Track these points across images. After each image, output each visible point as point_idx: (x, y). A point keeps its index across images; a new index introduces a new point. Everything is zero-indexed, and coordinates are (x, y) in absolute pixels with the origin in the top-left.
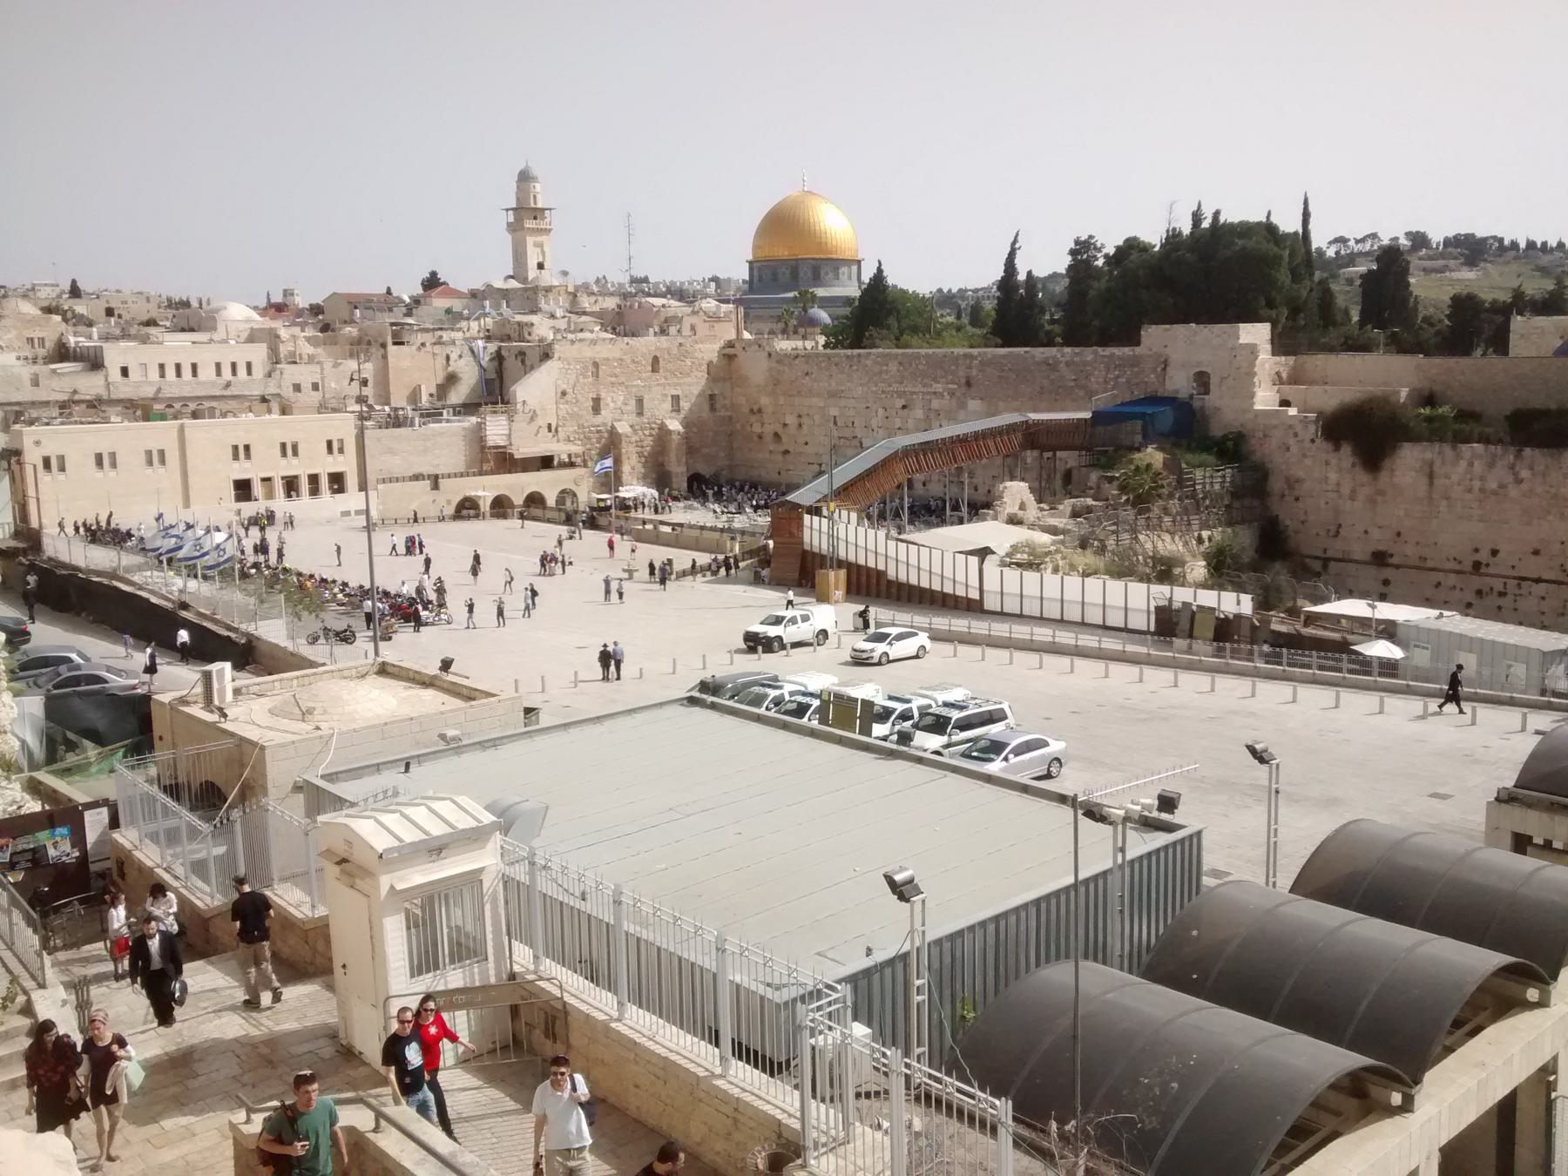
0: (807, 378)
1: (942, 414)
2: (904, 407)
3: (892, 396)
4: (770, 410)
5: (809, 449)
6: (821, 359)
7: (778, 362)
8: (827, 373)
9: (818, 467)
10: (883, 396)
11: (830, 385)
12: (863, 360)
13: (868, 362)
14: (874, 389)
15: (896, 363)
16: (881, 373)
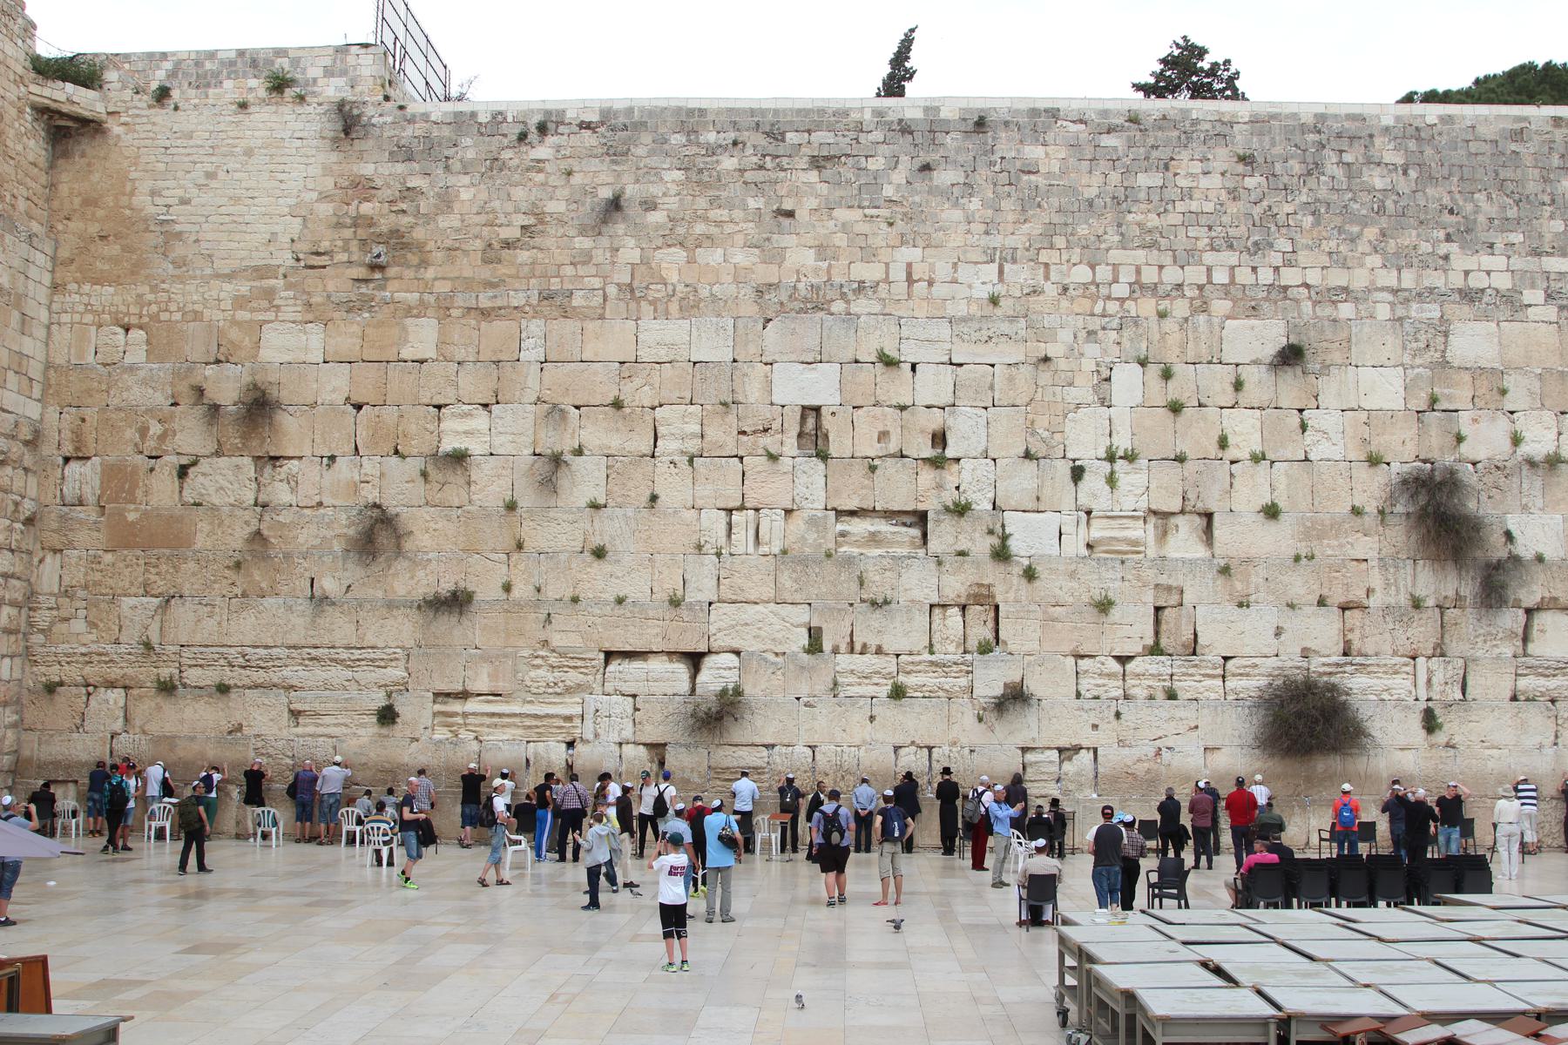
0: (620, 228)
1: (1519, 392)
2: (1291, 356)
3: (1204, 308)
4: (335, 385)
5: (599, 581)
6: (711, 137)
7: (404, 153)
8: (753, 203)
9: (681, 669)
10: (1146, 307)
11: (775, 257)
12: (1005, 145)
13: (1046, 156)
14: (1082, 274)
15: (1222, 158)
16: (1122, 201)
